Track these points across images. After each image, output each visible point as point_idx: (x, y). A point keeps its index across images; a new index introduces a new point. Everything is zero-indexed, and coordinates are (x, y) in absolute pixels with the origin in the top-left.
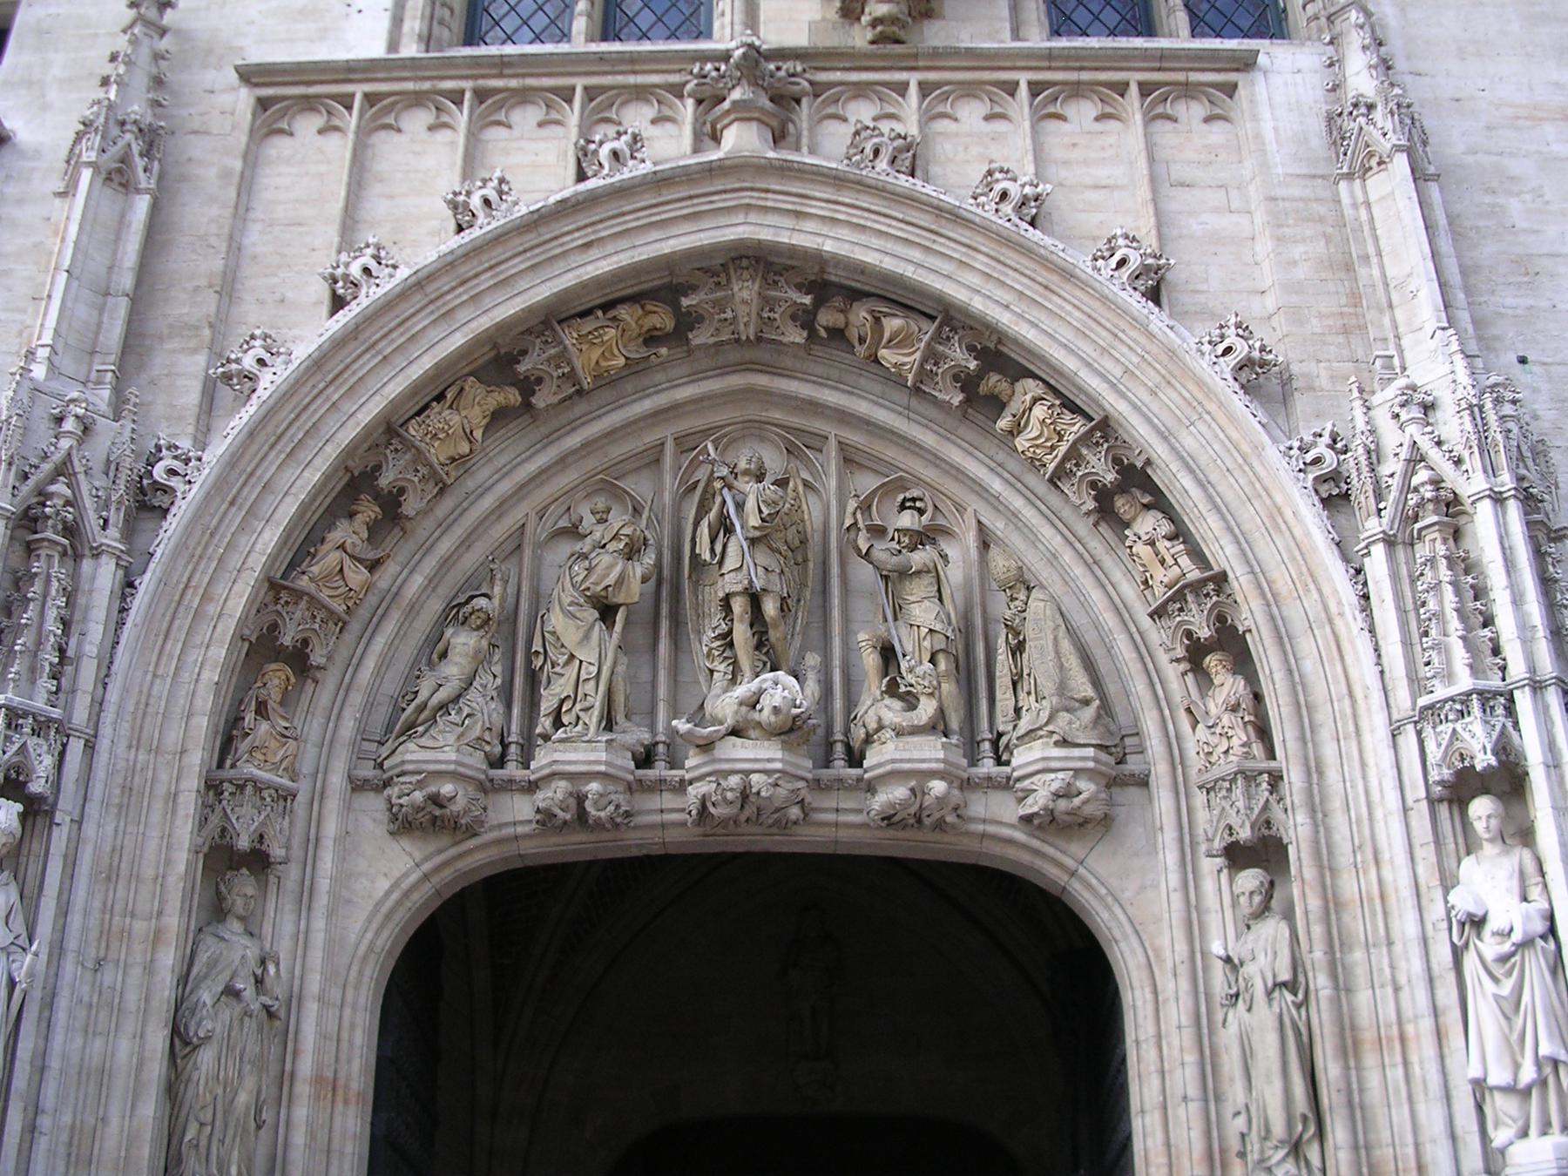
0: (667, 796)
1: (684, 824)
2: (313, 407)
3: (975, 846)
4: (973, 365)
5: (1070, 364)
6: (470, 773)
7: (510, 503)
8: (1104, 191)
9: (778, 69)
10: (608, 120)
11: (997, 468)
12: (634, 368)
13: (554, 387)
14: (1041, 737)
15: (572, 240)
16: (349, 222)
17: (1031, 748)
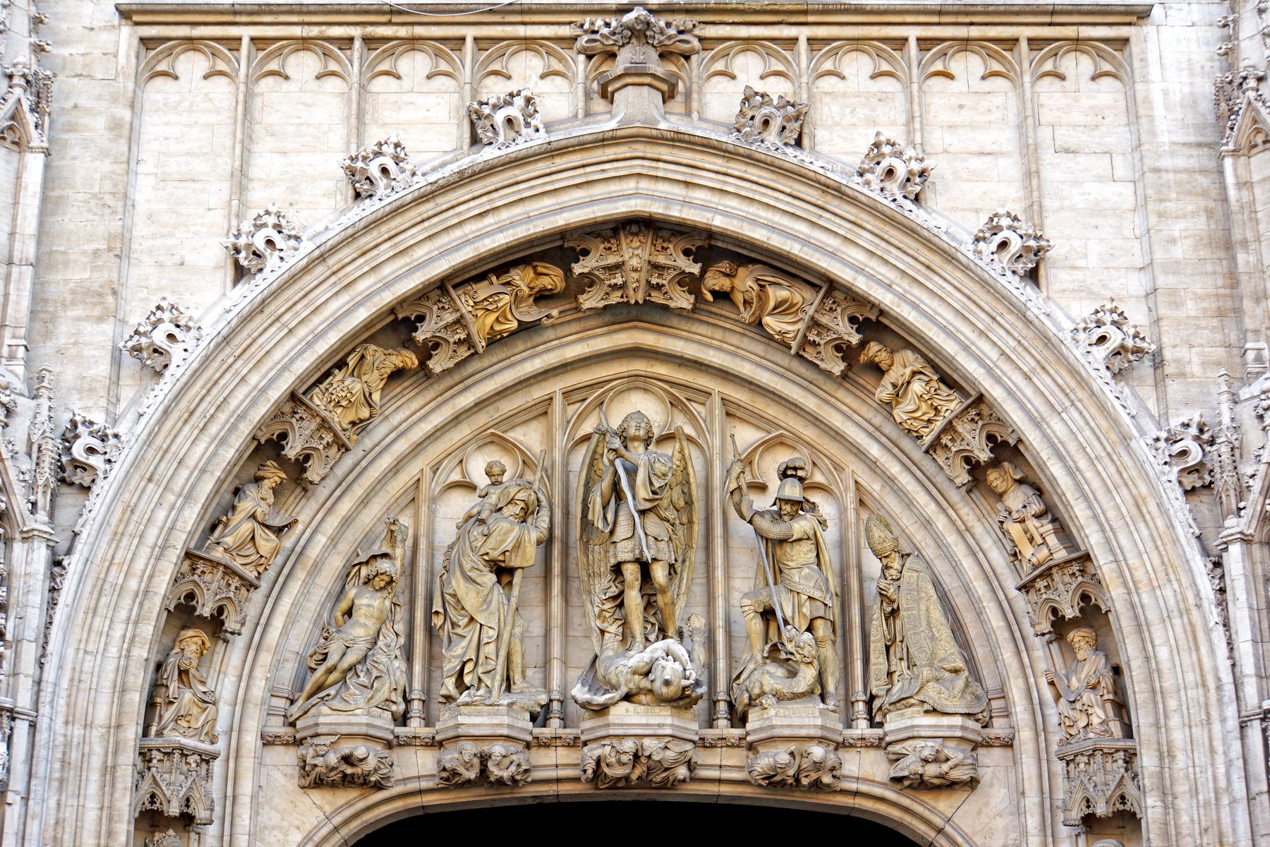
0: (562, 752)
1: (576, 780)
2: (222, 382)
5: (950, 347)
6: (379, 734)
8: (989, 158)
9: (668, 25)
11: (875, 433)
12: (526, 328)
13: (451, 352)
16: (244, 182)
17: (903, 715)
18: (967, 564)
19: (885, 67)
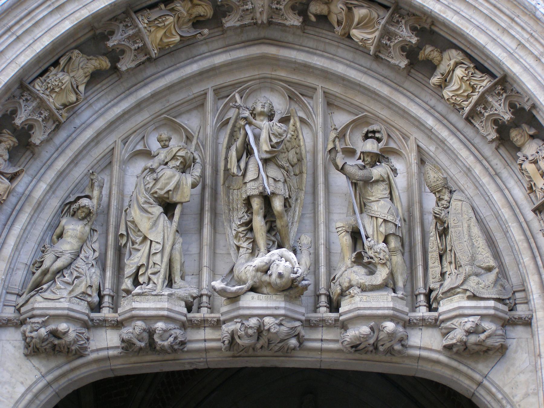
0: (208, 330)
1: (219, 349)
3: (413, 364)
4: (414, 40)
5: (481, 39)
7: (104, 134)
11: (430, 110)
13: (133, 55)
14: (458, 293)
17: (452, 300)
18: (496, 197)
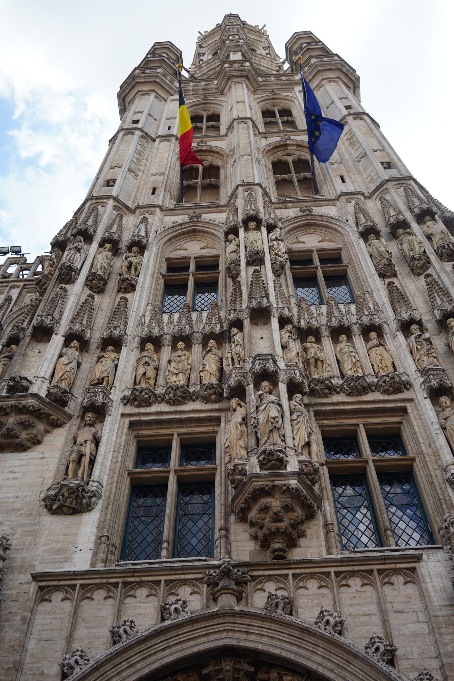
8: (367, 617)
9: (238, 571)
10: (173, 594)
15: (159, 647)
16: (71, 639)
19: (323, 584)
